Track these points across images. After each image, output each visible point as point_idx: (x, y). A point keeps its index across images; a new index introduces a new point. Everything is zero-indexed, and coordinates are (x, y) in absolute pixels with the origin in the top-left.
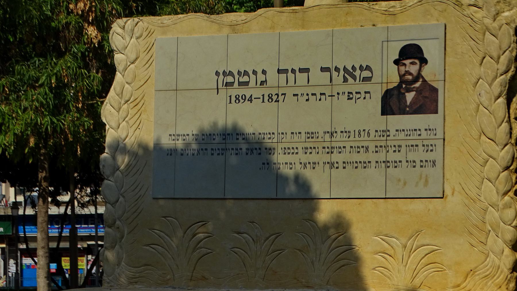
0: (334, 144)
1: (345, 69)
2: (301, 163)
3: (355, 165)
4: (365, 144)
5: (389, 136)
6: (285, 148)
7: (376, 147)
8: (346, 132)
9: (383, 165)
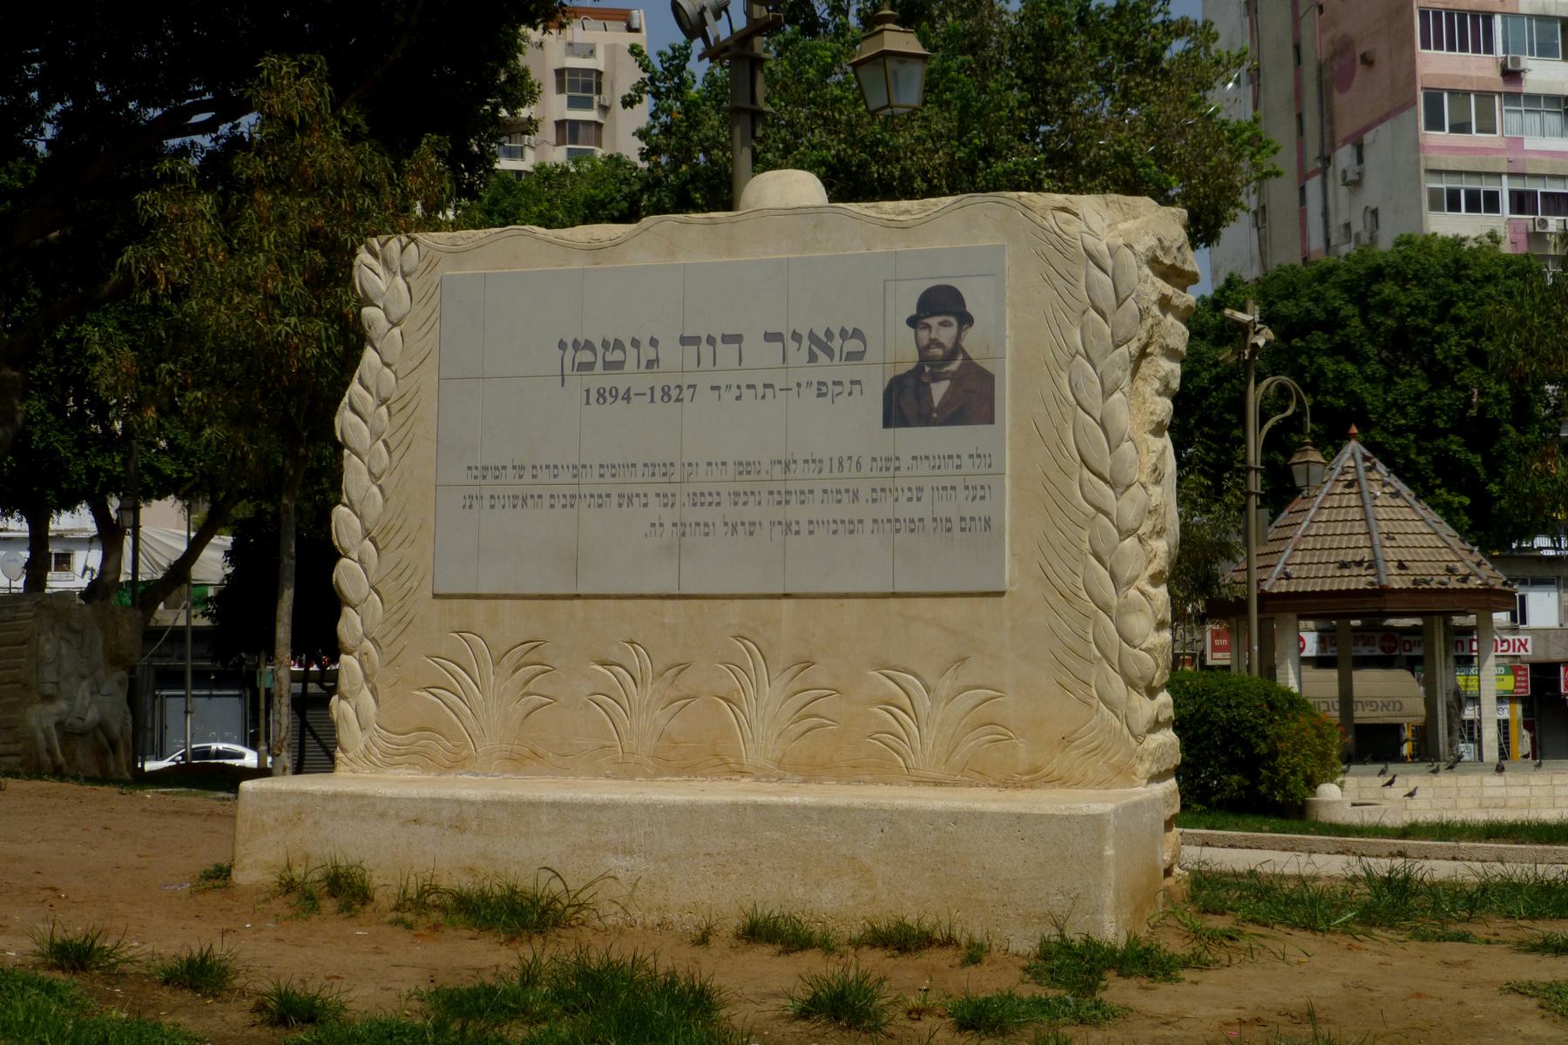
0: (791, 486)
1: (812, 335)
2: (726, 524)
3: (833, 527)
4: (852, 485)
5: (897, 469)
6: (695, 494)
7: (874, 490)
8: (814, 461)
9: (887, 526)
